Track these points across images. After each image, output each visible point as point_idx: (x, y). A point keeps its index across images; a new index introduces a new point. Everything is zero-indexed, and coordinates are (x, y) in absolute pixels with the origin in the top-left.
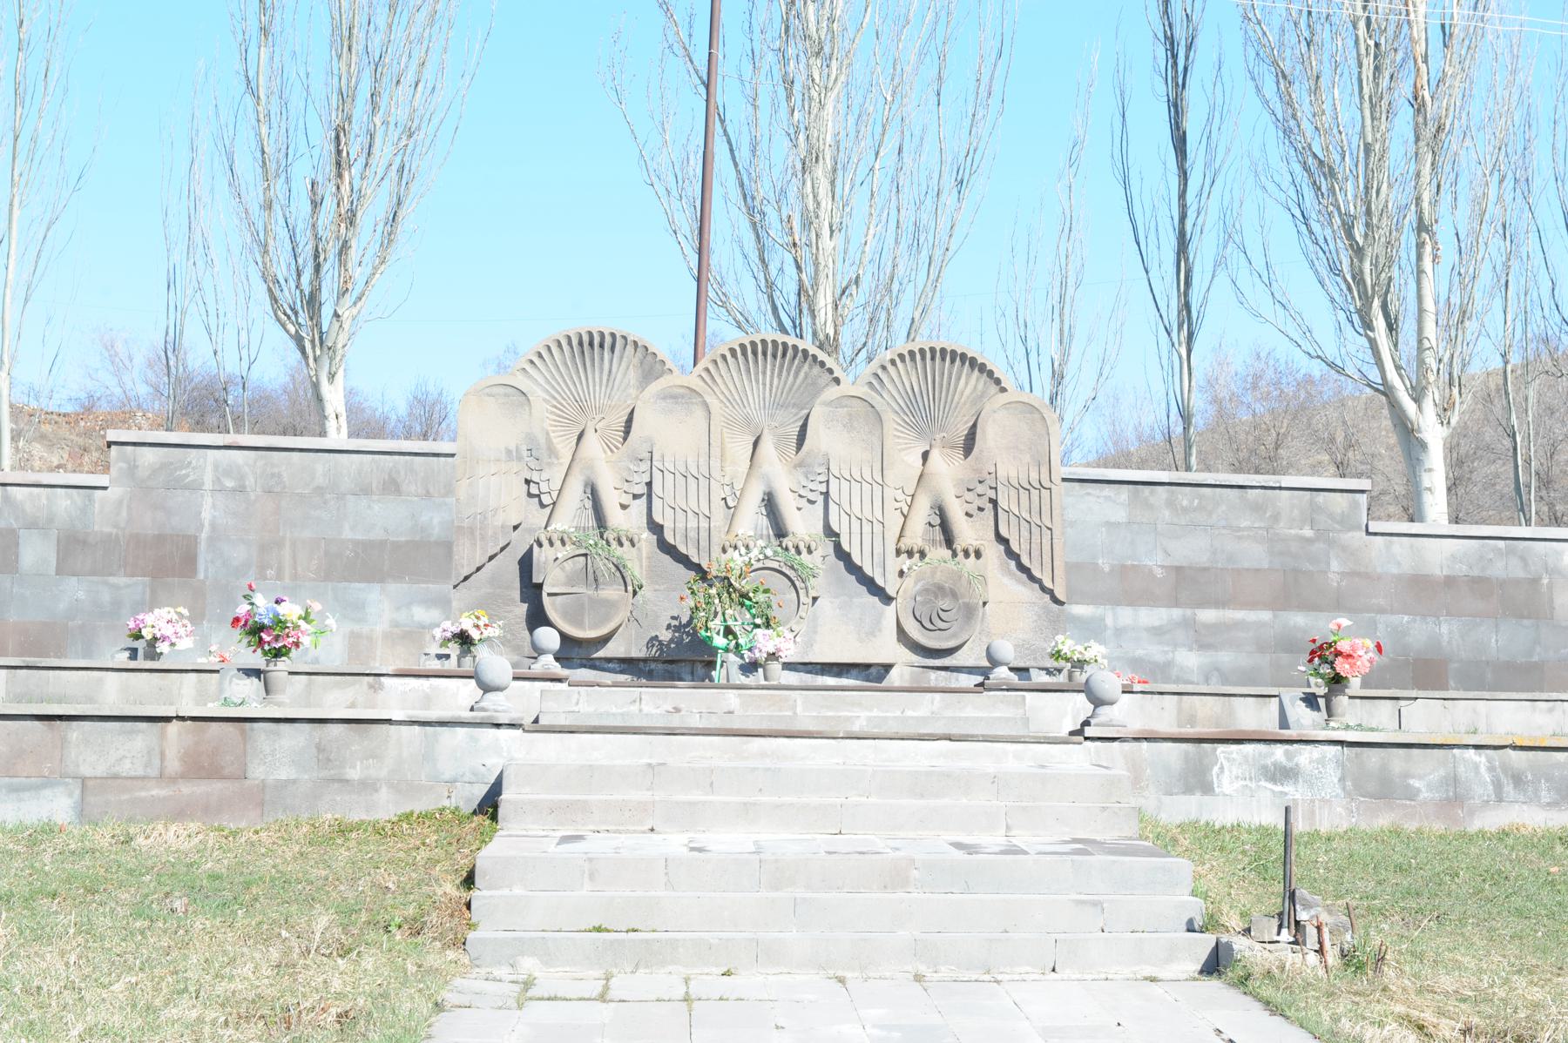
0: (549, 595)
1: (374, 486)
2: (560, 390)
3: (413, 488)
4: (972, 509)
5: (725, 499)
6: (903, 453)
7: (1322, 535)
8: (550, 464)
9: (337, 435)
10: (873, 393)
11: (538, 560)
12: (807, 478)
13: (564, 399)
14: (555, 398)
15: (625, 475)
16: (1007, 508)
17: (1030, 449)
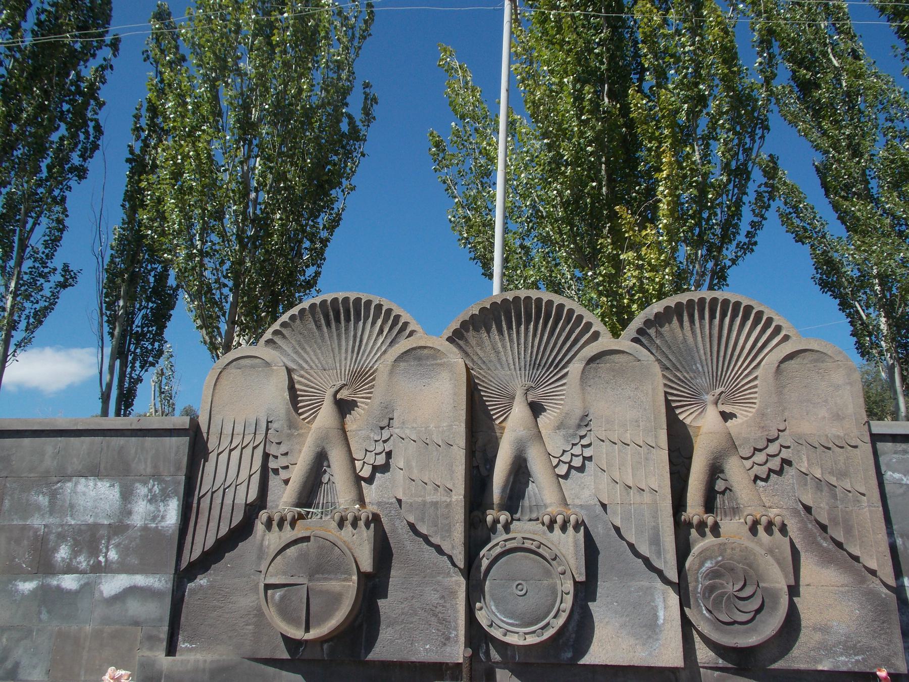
0: (267, 587)
1: (102, 466)
2: (308, 359)
3: (142, 467)
4: (762, 471)
5: (478, 467)
6: (678, 411)
8: (290, 436)
10: (638, 346)
11: (261, 544)
12: (568, 441)
13: (312, 368)
14: (302, 368)
15: (365, 445)
16: (803, 470)
17: (826, 401)
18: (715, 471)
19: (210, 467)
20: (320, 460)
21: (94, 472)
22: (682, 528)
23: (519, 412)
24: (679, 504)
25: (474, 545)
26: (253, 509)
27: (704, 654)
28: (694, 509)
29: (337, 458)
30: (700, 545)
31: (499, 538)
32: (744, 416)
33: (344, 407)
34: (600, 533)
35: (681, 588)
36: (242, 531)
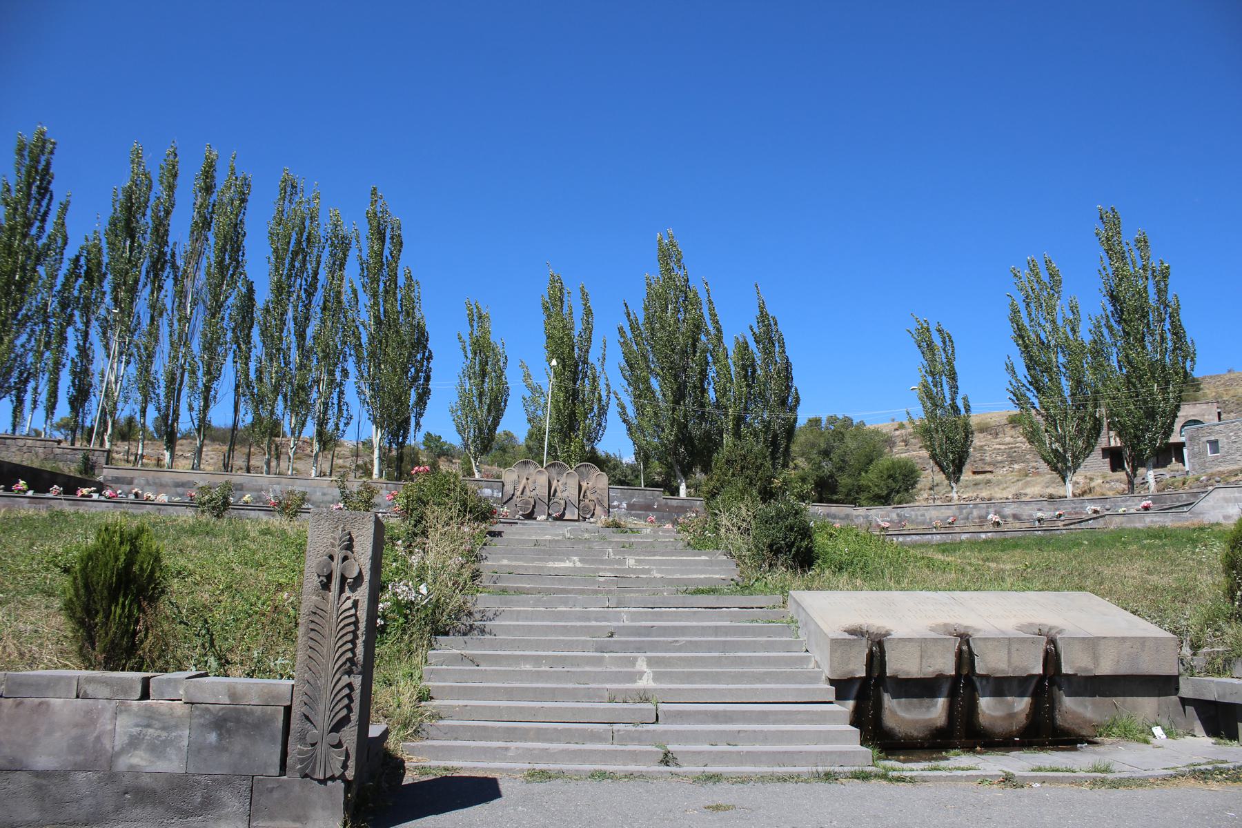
7: (654, 498)
9: (477, 476)
18: (585, 492)
19: (505, 488)
20: (524, 487)
21: (487, 487)
22: (579, 501)
23: (556, 481)
24: (579, 497)
25: (549, 500)
26: (513, 495)
27: (581, 518)
28: (581, 498)
29: (527, 487)
30: (582, 503)
31: (552, 501)
32: (590, 483)
33: (528, 479)
34: (567, 501)
35: (578, 509)
36: (511, 498)
